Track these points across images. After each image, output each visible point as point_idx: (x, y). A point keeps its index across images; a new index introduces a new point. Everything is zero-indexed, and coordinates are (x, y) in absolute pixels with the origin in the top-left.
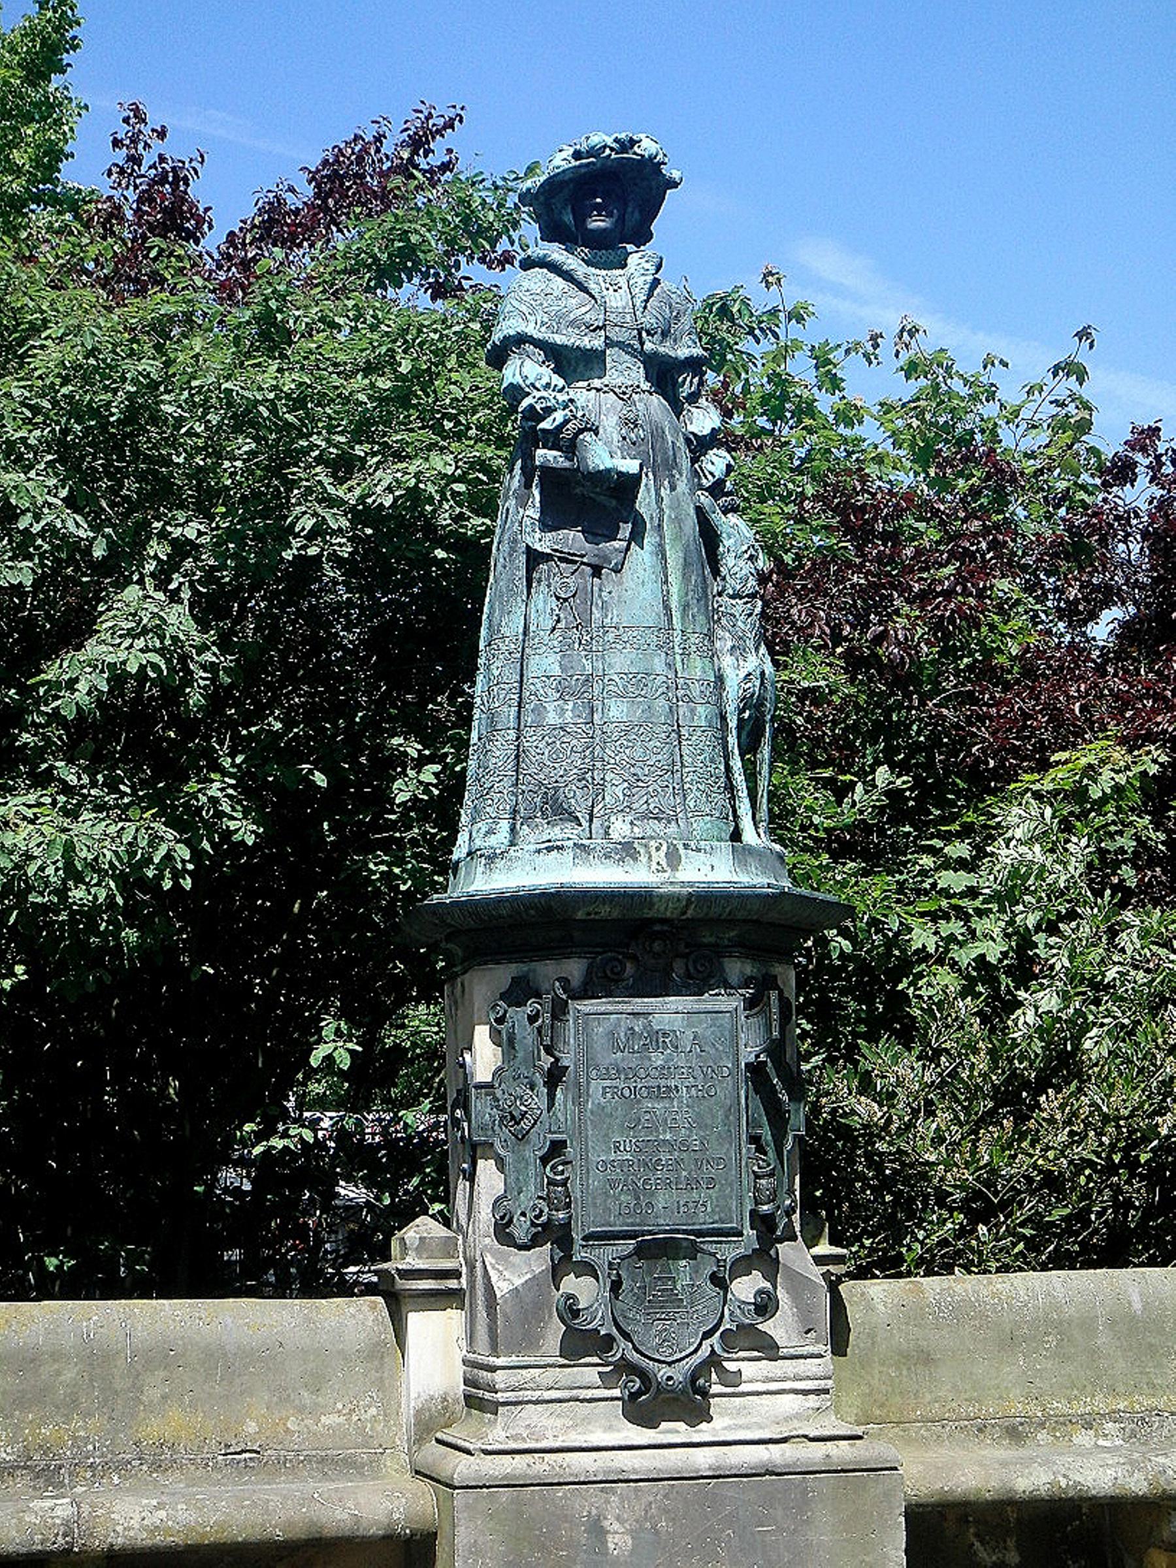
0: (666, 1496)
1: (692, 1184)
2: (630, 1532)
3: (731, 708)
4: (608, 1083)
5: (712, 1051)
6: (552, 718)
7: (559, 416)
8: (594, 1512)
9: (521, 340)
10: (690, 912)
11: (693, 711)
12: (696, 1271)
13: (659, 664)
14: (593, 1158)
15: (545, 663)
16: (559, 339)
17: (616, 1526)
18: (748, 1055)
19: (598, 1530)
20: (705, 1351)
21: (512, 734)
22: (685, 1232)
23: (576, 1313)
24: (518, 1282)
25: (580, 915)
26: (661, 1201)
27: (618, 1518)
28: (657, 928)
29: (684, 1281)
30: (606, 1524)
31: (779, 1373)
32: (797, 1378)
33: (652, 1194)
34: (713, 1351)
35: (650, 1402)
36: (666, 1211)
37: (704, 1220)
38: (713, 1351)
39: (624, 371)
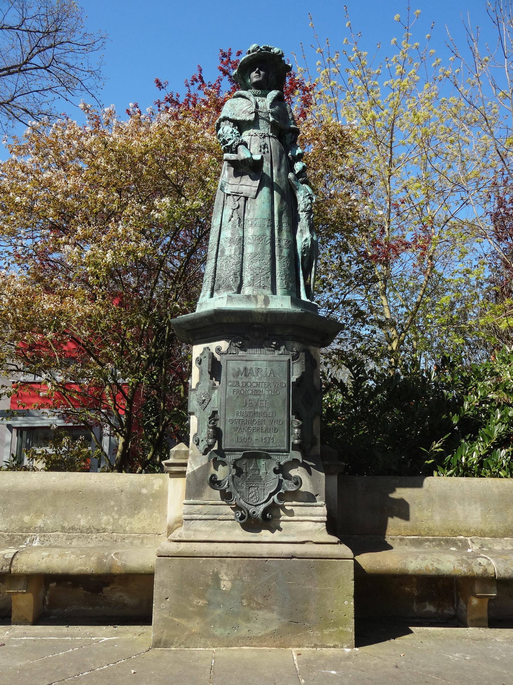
0: (247, 565)
1: (267, 431)
2: (231, 580)
3: (299, 251)
4: (235, 388)
5: (278, 376)
6: (227, 253)
7: (232, 141)
8: (216, 570)
9: (225, 119)
10: (268, 320)
11: (281, 251)
12: (267, 467)
13: (268, 233)
14: (228, 418)
15: (227, 234)
16: (238, 118)
17: (225, 577)
18: (294, 379)
19: (217, 579)
20: (271, 501)
21: (214, 260)
22: (264, 450)
23: (219, 482)
24: (195, 468)
25: (225, 321)
26: (255, 437)
27: (226, 574)
28: (256, 326)
29: (263, 471)
30: (220, 576)
31: (304, 512)
32: (312, 515)
33: (251, 434)
34: (273, 502)
35: (251, 524)
36: (257, 441)
37: (271, 446)
38: (273, 502)
39: (264, 128)
